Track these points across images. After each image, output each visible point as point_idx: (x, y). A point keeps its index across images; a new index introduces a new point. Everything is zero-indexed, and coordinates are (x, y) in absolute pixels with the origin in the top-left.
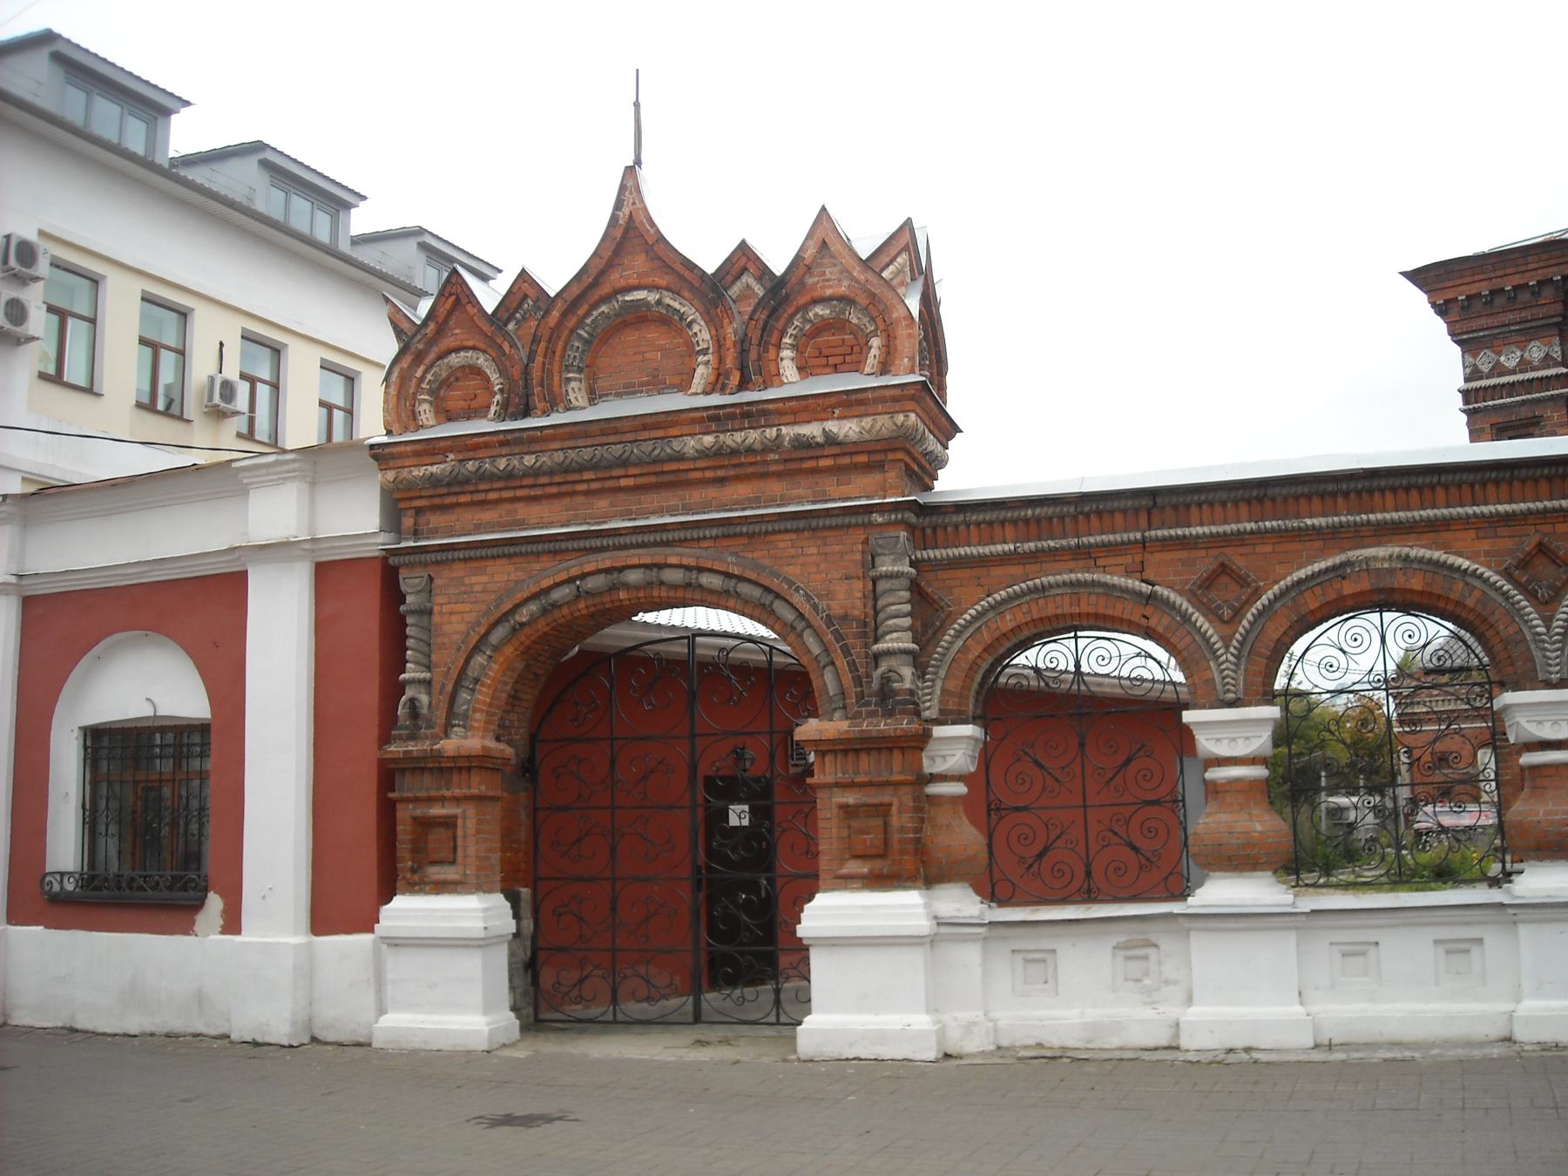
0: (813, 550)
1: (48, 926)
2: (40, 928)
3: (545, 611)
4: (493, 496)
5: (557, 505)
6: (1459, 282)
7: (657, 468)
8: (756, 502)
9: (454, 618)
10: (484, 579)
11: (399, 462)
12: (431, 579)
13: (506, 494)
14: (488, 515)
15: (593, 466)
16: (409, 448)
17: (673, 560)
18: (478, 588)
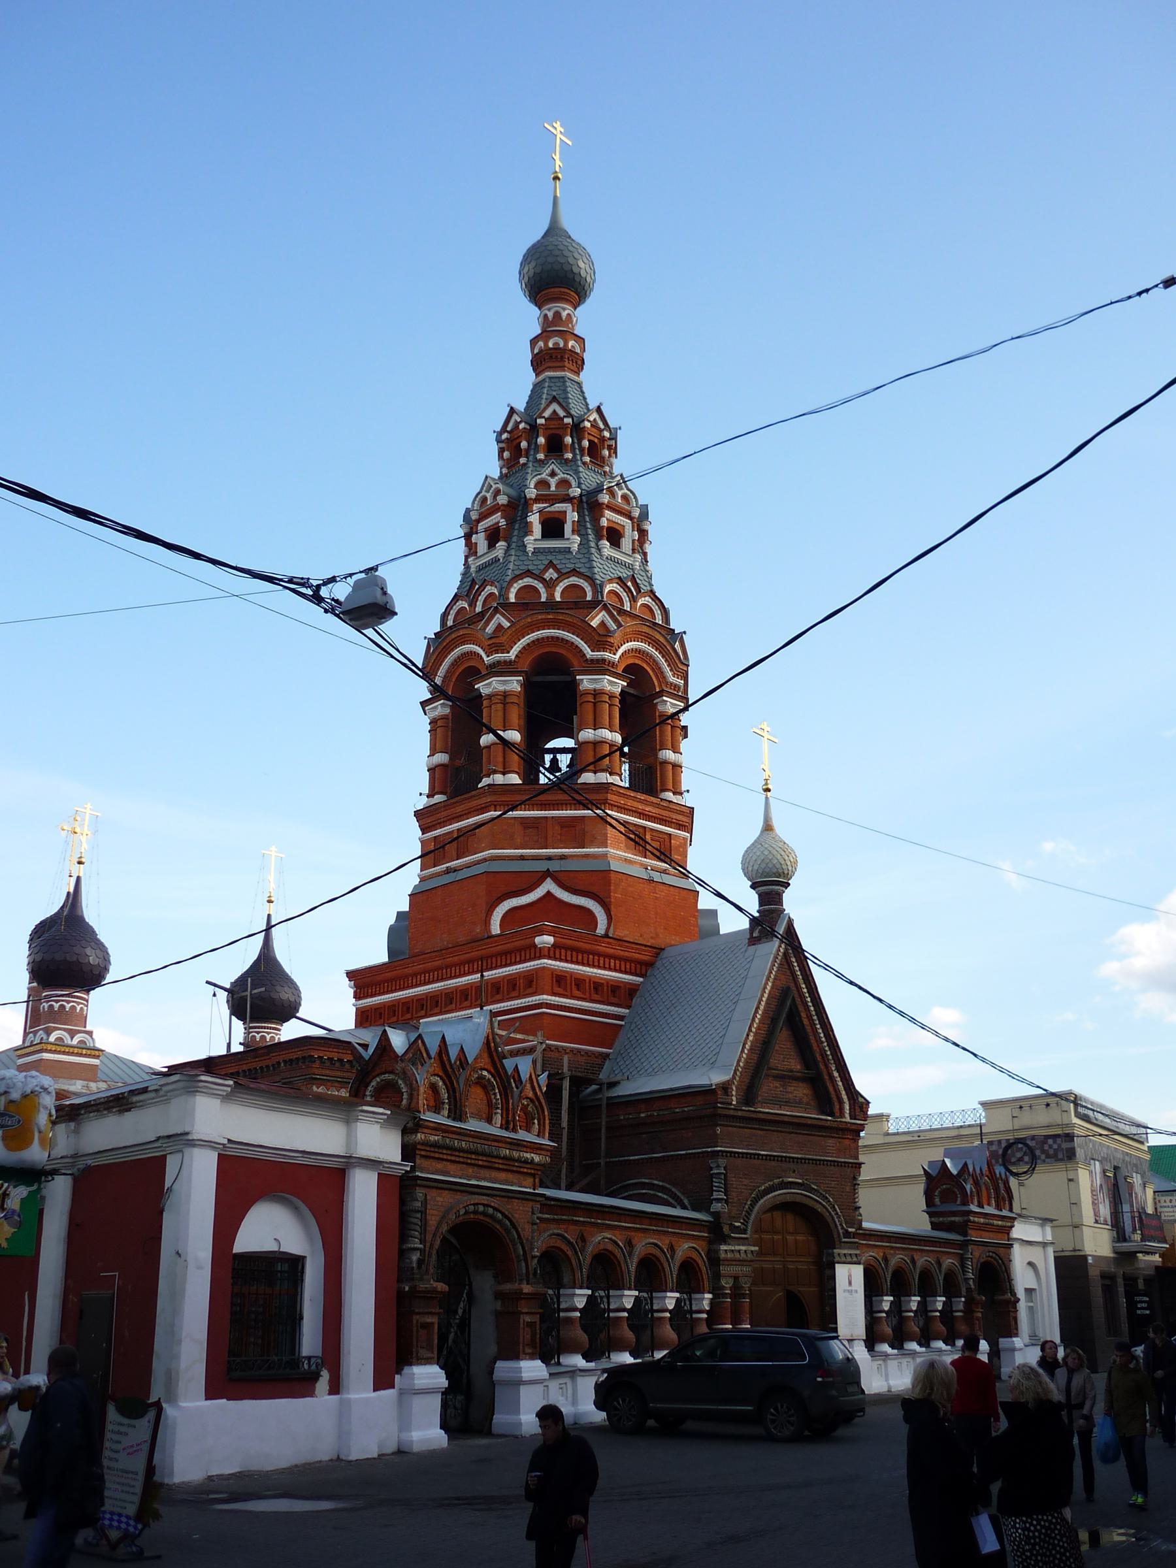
0: (521, 1208)
1: (229, 1399)
2: (224, 1401)
4: (445, 1157)
6: (327, 1049)
7: (489, 1159)
8: (507, 1182)
11: (426, 1131)
14: (440, 1166)
16: (432, 1125)
17: (493, 1204)
18: (440, 1203)
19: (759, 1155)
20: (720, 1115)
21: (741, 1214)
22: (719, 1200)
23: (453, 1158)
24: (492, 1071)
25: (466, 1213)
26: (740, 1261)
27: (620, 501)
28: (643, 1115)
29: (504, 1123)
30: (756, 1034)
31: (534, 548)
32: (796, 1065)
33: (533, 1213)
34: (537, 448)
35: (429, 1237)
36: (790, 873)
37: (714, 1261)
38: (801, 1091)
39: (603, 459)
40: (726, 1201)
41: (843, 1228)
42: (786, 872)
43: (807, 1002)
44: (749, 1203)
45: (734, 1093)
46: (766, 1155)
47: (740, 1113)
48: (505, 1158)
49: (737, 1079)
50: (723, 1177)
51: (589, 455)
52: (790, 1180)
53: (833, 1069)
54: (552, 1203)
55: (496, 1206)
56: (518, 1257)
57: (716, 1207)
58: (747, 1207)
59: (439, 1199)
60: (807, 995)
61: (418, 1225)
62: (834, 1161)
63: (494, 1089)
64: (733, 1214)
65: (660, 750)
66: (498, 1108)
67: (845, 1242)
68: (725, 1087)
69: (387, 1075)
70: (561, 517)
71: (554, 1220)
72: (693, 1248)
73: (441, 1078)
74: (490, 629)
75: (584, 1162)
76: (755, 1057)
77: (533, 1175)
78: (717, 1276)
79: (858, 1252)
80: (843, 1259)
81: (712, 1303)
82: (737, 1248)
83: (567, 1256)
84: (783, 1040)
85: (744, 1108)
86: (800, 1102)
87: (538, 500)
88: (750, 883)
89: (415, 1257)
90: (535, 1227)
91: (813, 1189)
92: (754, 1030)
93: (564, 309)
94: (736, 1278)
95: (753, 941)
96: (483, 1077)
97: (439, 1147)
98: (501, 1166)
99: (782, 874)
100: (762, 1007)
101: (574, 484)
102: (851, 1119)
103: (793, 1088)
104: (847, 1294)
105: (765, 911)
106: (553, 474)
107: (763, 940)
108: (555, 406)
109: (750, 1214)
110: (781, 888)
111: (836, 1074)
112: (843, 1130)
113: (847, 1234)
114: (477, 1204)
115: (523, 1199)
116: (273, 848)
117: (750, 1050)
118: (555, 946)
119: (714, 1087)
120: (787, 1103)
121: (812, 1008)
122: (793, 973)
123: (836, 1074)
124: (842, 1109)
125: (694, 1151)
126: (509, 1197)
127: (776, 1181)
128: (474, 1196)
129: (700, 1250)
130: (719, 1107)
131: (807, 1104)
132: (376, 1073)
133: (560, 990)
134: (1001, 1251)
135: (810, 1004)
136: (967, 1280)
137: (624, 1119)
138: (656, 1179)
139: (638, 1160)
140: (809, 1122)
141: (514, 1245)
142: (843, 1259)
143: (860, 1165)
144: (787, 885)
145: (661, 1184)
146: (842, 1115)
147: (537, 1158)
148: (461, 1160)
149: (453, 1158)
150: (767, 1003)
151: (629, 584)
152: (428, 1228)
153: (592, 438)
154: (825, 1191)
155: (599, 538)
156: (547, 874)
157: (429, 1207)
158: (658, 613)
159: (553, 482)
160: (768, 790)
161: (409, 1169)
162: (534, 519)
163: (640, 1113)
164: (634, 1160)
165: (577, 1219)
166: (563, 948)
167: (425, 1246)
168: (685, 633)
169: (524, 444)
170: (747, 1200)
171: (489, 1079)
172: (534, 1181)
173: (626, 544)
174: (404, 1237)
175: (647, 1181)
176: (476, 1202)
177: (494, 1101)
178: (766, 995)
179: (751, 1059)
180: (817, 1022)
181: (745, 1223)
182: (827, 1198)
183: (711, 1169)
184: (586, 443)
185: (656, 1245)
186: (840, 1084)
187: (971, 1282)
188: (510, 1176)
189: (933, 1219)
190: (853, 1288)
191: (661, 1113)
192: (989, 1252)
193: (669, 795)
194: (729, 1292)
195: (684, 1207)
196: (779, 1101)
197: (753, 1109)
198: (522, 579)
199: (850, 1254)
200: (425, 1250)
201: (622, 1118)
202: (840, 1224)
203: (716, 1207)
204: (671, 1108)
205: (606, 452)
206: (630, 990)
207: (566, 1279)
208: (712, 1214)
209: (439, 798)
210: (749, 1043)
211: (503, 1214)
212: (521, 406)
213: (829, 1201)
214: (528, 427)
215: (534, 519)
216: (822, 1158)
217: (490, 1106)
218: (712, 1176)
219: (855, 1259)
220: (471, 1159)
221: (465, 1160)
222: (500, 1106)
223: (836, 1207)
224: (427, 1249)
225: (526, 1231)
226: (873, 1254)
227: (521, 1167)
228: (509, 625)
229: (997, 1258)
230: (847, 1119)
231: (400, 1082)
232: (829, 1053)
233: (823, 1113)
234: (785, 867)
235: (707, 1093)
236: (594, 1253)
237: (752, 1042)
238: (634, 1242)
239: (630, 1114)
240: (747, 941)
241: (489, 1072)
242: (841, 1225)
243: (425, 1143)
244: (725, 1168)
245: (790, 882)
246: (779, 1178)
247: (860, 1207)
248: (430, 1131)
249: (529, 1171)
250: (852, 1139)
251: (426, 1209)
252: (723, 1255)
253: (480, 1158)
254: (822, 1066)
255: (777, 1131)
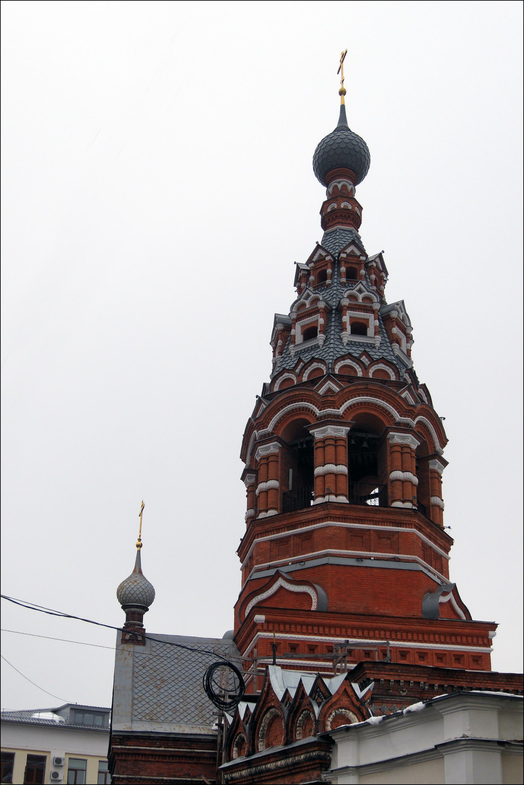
31: (348, 341)
34: (340, 275)
65: (432, 496)
70: (364, 322)
74: (321, 392)
87: (351, 308)
101: (375, 299)
108: (352, 248)
159: (360, 297)
168: (444, 419)
169: (329, 271)
198: (344, 360)
214: (333, 260)
228: (339, 390)
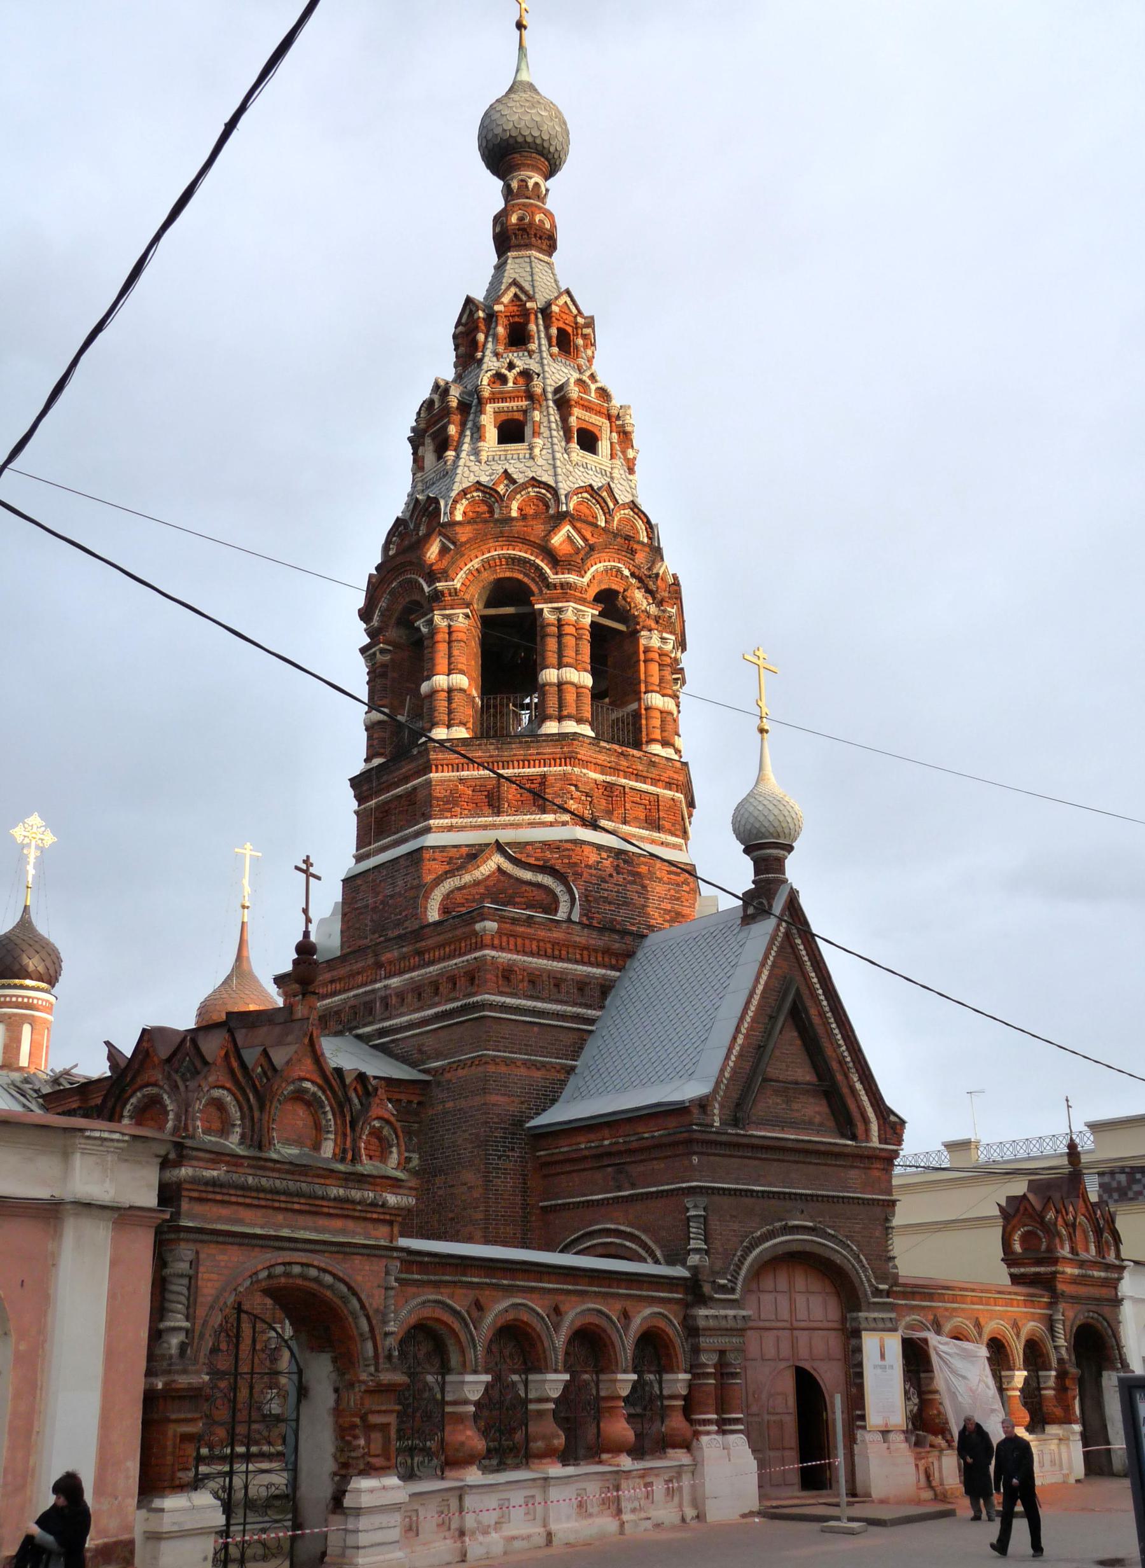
0: (367, 1268)
3: (343, 1298)
4: (234, 1199)
5: (260, 1213)
7: (311, 1202)
8: (343, 1232)
9: (209, 1284)
10: (226, 1258)
11: (195, 1163)
12: (197, 1253)
13: (241, 1200)
15: (286, 1193)
17: (316, 1263)
19: (753, 1191)
20: (697, 1141)
21: (728, 1268)
22: (697, 1251)
23: (248, 1201)
24: (319, 1081)
25: (270, 1276)
26: (727, 1330)
27: (593, 394)
28: (606, 1142)
29: (337, 1151)
30: (747, 1036)
32: (804, 1074)
33: (387, 1273)
35: (201, 1312)
36: (792, 833)
37: (692, 1331)
38: (814, 1109)
39: (577, 347)
40: (707, 1252)
41: (871, 1285)
42: (787, 831)
43: (817, 995)
44: (739, 1253)
45: (716, 1111)
46: (763, 1192)
47: (724, 1138)
48: (336, 1199)
49: (722, 1093)
50: (702, 1220)
51: (559, 345)
52: (796, 1223)
53: (855, 1079)
54: (426, 1259)
55: (323, 1265)
56: (361, 1335)
57: (694, 1259)
58: (736, 1259)
59: (220, 1257)
60: (818, 986)
61: (182, 1294)
62: (858, 1198)
63: (323, 1107)
64: (717, 1269)
66: (328, 1132)
67: (875, 1303)
68: (703, 1104)
69: (149, 1089)
71: (430, 1282)
72: (660, 1313)
73: (228, 1090)
75: (541, 1204)
76: (747, 1066)
77: (391, 1223)
78: (696, 1350)
79: (893, 1315)
80: (873, 1325)
81: (690, 1386)
82: (723, 1312)
83: (453, 1330)
84: (789, 1043)
85: (729, 1131)
86: (811, 1123)
87: (493, 400)
88: (743, 847)
89: (175, 1341)
90: (392, 1293)
91: (830, 1234)
92: (744, 1031)
93: (530, 178)
94: (722, 1353)
95: (748, 919)
96: (306, 1090)
97: (222, 1186)
98: (332, 1211)
99: (782, 834)
100: (755, 1002)
102: (880, 1143)
103: (800, 1105)
104: (879, 1371)
105: (761, 881)
106: (511, 366)
107: (759, 918)
109: (740, 1269)
110: (782, 852)
111: (859, 1086)
112: (869, 1157)
113: (877, 1292)
114: (290, 1264)
115: (368, 1255)
116: (248, 846)
117: (740, 1056)
118: (499, 932)
119: (687, 1104)
120: (794, 1125)
121: (825, 1003)
122: (798, 958)
123: (859, 1086)
124: (867, 1131)
125: (666, 1187)
126: (345, 1253)
127: (778, 1224)
128: (282, 1253)
129: (671, 1317)
130: (696, 1131)
131: (821, 1124)
132: (136, 1086)
133: (507, 990)
134: (1106, 1311)
135: (822, 997)
136: (1056, 1348)
137: (586, 1148)
138: (623, 1224)
139: (603, 1200)
140: (822, 1148)
141: (356, 1318)
142: (873, 1325)
143: (893, 1203)
144: (790, 848)
145: (628, 1230)
146: (868, 1138)
147: (392, 1199)
148: (263, 1203)
149: (248, 1201)
150: (763, 996)
151: (604, 494)
152: (200, 1299)
153: (561, 325)
154: (847, 1237)
155: (568, 439)
156: (499, 847)
157: (202, 1269)
158: (640, 525)
160: (762, 731)
161: (168, 1216)
162: (488, 421)
163: (604, 1139)
164: (598, 1201)
165: (469, 1279)
166: (512, 935)
167: (193, 1324)
170: (736, 1250)
171: (314, 1094)
172: (392, 1231)
173: (604, 446)
174: (159, 1310)
175: (613, 1226)
176: (287, 1260)
177: (324, 1122)
178: (760, 987)
179: (740, 1068)
180: (832, 1020)
181: (734, 1281)
182: (848, 1246)
183: (688, 1210)
184: (554, 331)
185: (599, 1311)
186: (865, 1098)
187: (1063, 1351)
188: (350, 1224)
189: (1012, 1270)
190: (887, 1362)
191: (627, 1139)
192: (1089, 1311)
193: (656, 748)
194: (713, 1370)
195: (657, 1262)
196: (780, 1122)
197: (742, 1132)
199: (883, 1319)
200: (193, 1331)
201: (583, 1146)
202: (866, 1279)
203: (694, 1259)
204: (638, 1134)
205: (580, 342)
206: (602, 986)
207: (454, 1360)
208: (689, 1268)
209: (377, 761)
210: (737, 1048)
211: (334, 1276)
212: (479, 295)
213: (852, 1250)
215: (488, 421)
216: (841, 1194)
217: (318, 1127)
218: (688, 1219)
219: (889, 1325)
220: (280, 1201)
221: (269, 1203)
222: (332, 1129)
223: (862, 1257)
224: (198, 1328)
225: (375, 1299)
226: (918, 1317)
227: (366, 1212)
229: (1101, 1319)
230: (875, 1142)
231: (165, 1097)
232: (848, 1059)
233: (843, 1136)
234: (784, 825)
235: (678, 1110)
236: (499, 1325)
237: (742, 1047)
238: (563, 1308)
239: (593, 1142)
240: (739, 921)
241: (313, 1082)
242: (869, 1281)
243: (194, 1181)
244: (705, 1209)
245: (794, 844)
246: (781, 1220)
247: (894, 1258)
248: (201, 1164)
249: (382, 1217)
250: (883, 1169)
251: (197, 1273)
252: (702, 1323)
253: (295, 1199)
254: (839, 1077)
255: (778, 1160)
